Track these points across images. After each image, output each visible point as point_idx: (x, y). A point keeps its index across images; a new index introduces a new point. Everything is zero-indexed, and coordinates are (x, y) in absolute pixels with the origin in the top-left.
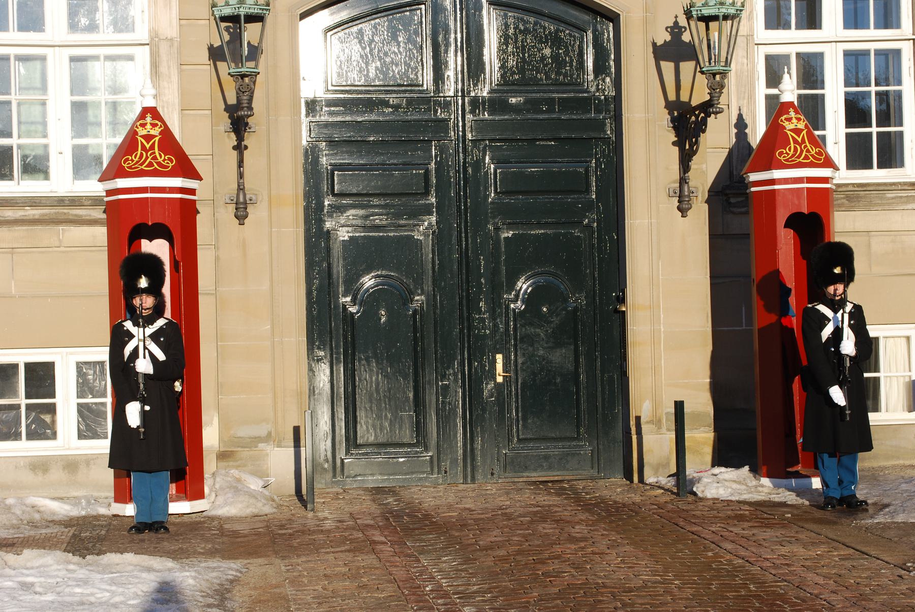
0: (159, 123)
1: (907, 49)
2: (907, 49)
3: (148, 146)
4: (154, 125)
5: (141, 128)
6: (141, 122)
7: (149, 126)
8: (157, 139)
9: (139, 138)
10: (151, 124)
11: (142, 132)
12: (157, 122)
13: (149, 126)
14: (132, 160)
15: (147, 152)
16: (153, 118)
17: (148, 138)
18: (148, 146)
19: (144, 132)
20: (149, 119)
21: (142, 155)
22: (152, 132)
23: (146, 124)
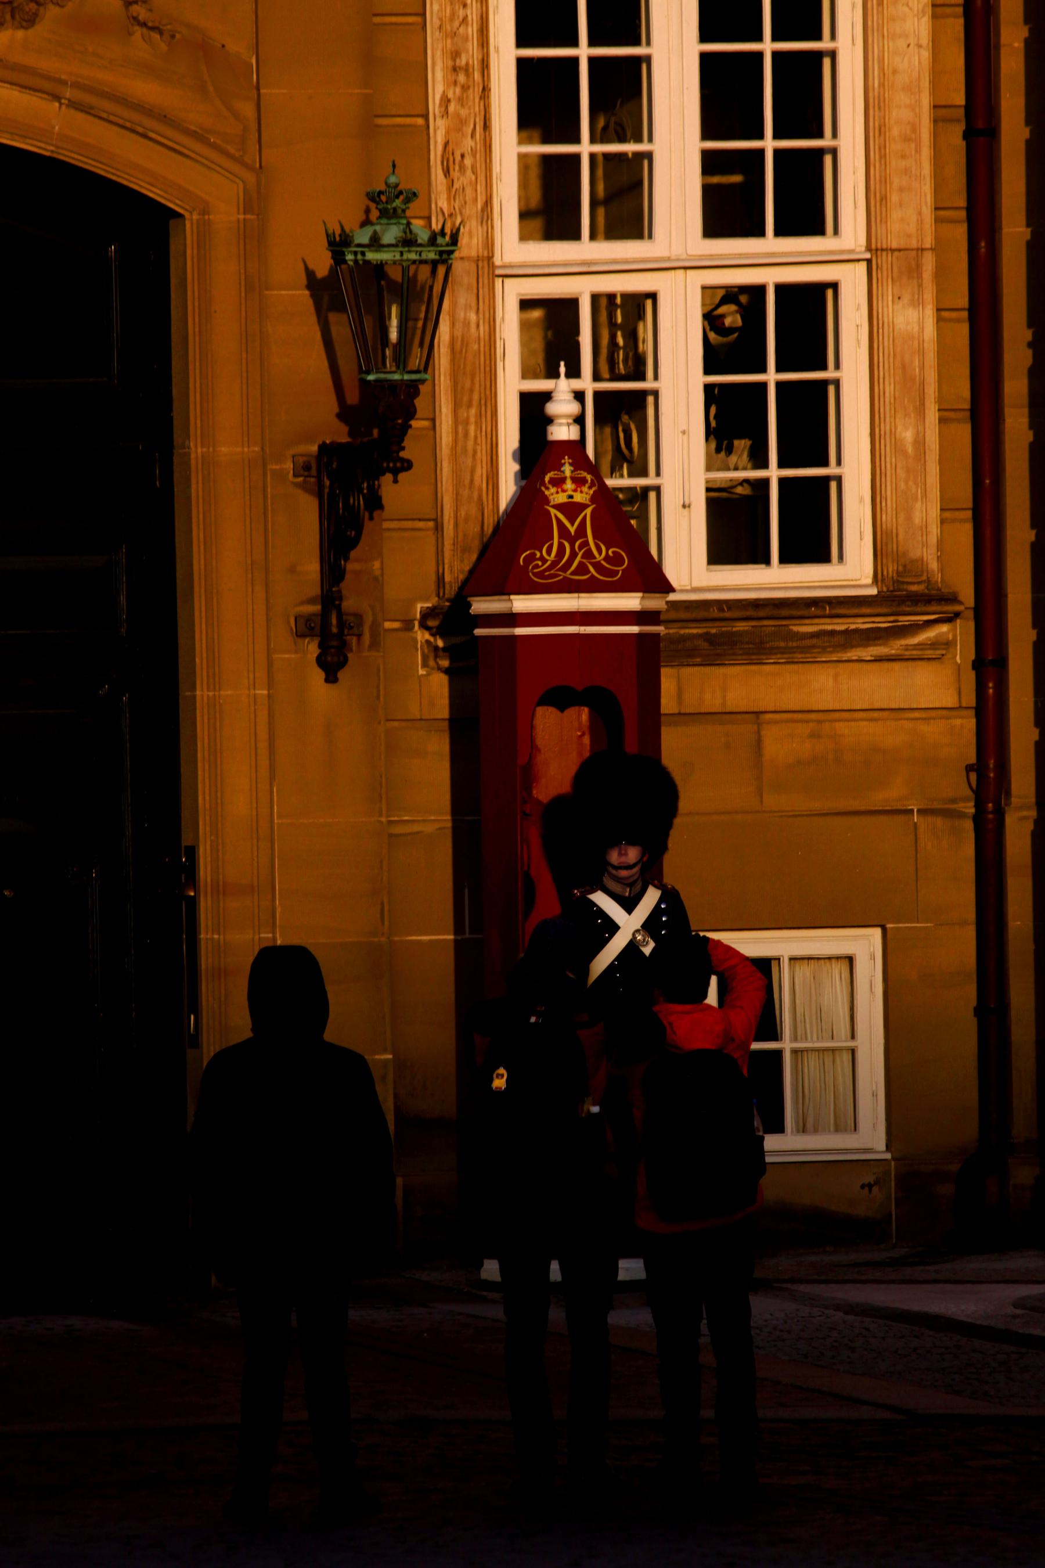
0: (589, 477)
1: (853, 282)
2: (853, 282)
3: (572, 530)
4: (579, 482)
5: (553, 490)
7: (569, 485)
8: (588, 511)
10: (574, 480)
12: (584, 474)
13: (569, 485)
16: (576, 467)
17: (571, 509)
18: (572, 530)
19: (561, 498)
21: (561, 547)
22: (579, 498)
23: (563, 480)
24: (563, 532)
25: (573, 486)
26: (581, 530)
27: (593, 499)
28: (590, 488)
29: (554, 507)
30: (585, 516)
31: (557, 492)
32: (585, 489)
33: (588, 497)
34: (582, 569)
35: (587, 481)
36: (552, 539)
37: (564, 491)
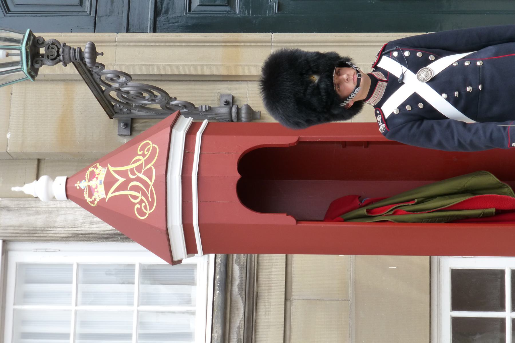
3: (121, 180)
6: (86, 197)
7: (93, 183)
8: (111, 169)
9: (110, 195)
11: (100, 194)
14: (142, 201)
15: (130, 180)
20: (83, 185)
24: (123, 187)
25: (95, 179)
26: (122, 174)
27: (104, 166)
28: (97, 168)
29: (107, 194)
30: (114, 171)
31: (98, 192)
32: (97, 171)
33: (103, 169)
34: (148, 173)
35: (93, 171)
36: (127, 195)
37: (96, 187)
